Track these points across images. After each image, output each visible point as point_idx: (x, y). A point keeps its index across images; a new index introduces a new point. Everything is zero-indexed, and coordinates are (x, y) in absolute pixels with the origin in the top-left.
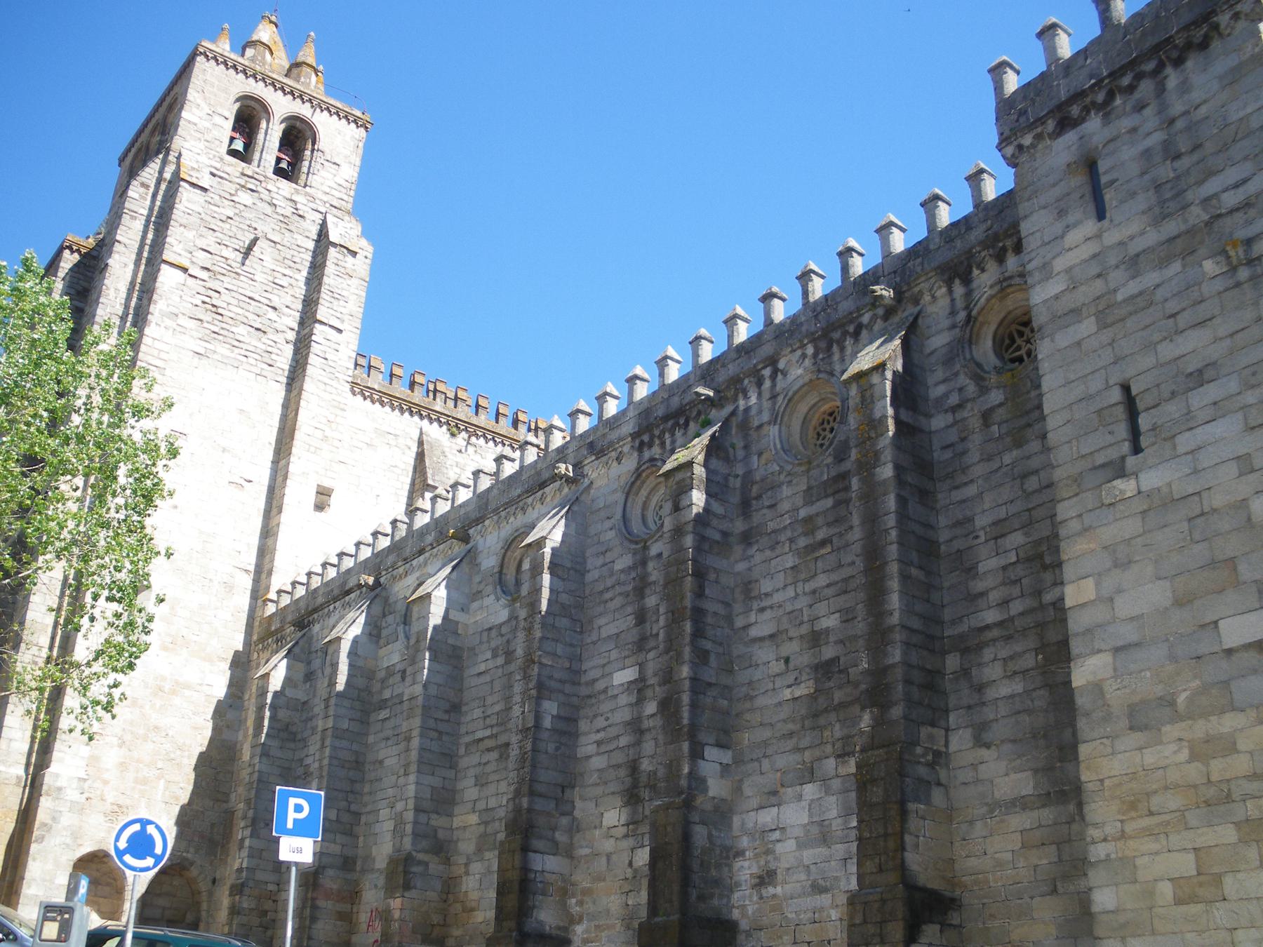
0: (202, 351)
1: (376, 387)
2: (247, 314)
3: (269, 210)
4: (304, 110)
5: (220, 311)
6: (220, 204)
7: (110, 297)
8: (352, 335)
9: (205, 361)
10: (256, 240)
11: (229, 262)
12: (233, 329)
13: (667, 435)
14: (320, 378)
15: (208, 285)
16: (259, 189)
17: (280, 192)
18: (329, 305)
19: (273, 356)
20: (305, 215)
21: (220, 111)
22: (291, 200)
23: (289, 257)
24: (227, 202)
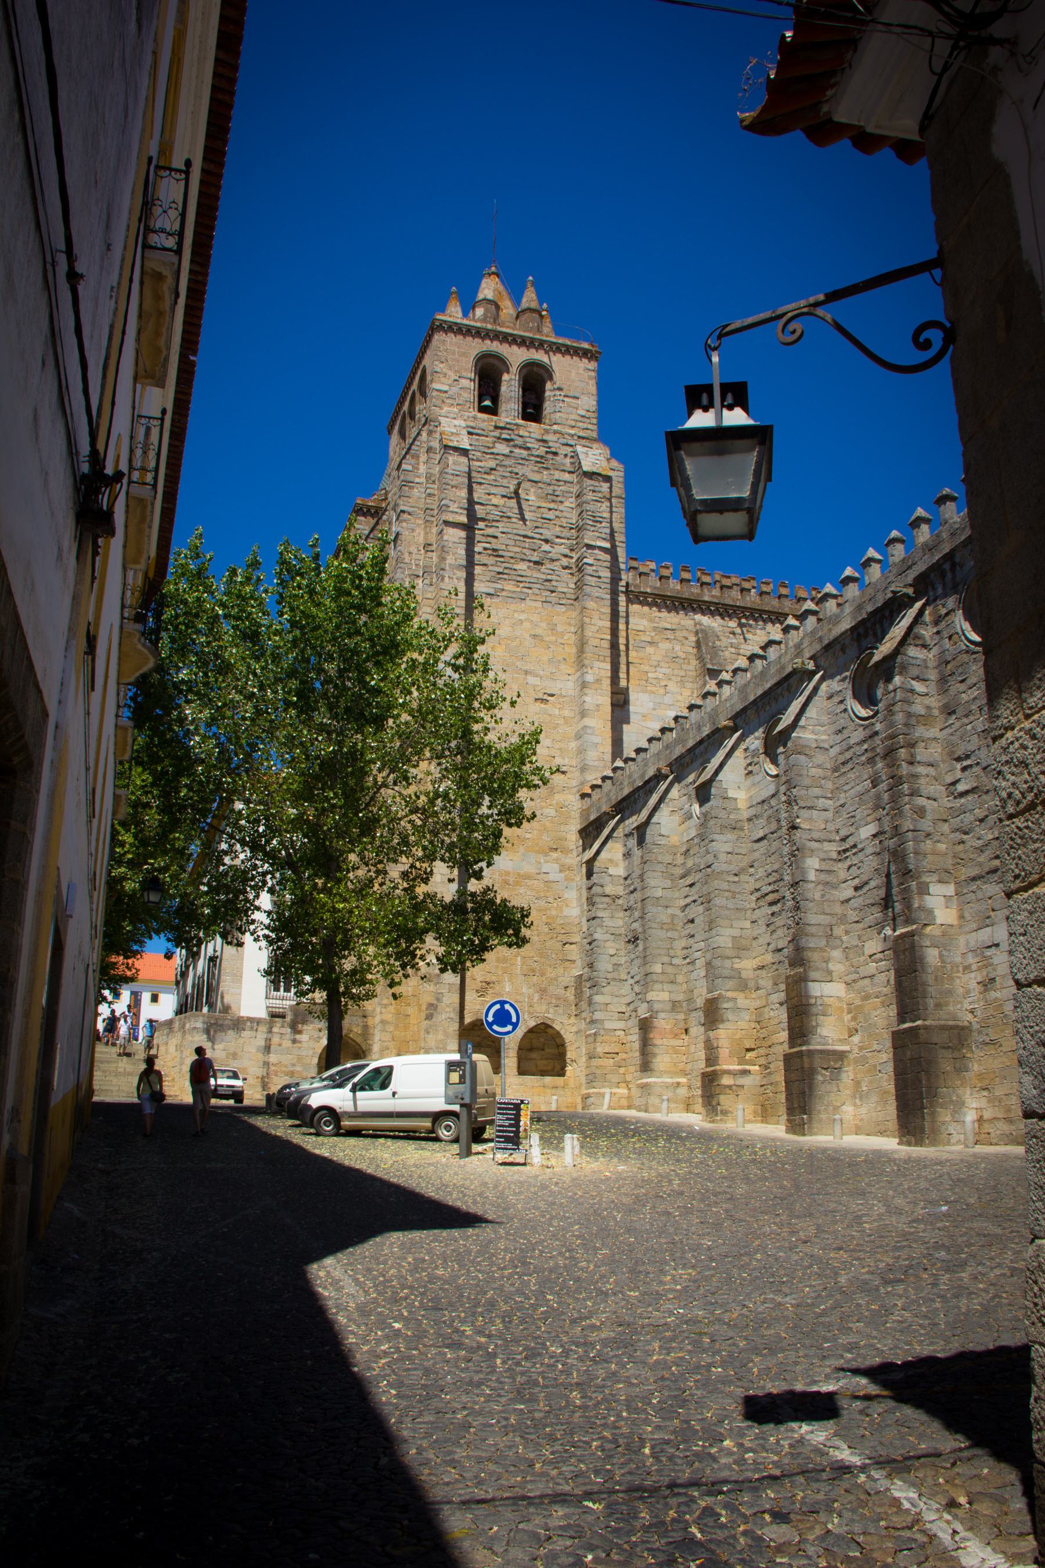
0: (492, 591)
1: (648, 590)
2: (524, 551)
4: (540, 356)
5: (500, 553)
7: (406, 560)
9: (495, 600)
10: (519, 484)
12: (515, 567)
13: (878, 626)
17: (533, 435)
18: (592, 529)
19: (554, 583)
20: (558, 451)
23: (551, 492)
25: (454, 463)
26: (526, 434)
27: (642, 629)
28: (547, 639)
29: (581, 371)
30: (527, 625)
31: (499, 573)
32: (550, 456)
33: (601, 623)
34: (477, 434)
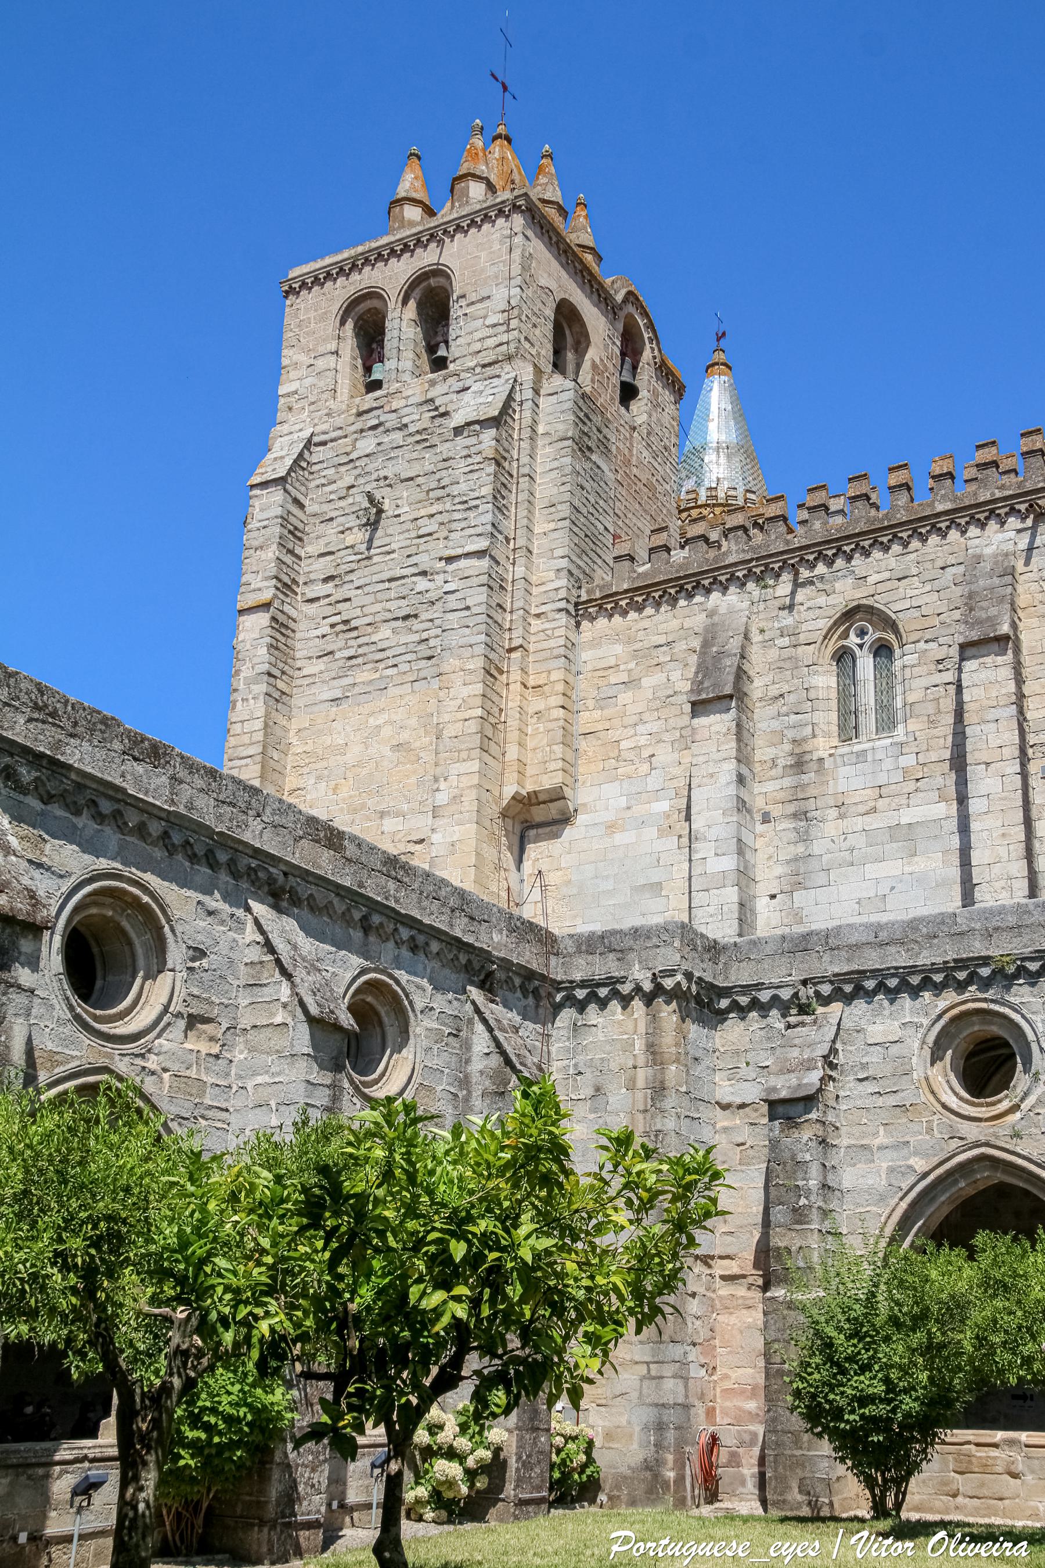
3: (397, 437)
4: (426, 258)
5: (354, 623)
6: (336, 477)
8: (556, 535)
9: (345, 705)
11: (356, 550)
12: (374, 638)
14: (463, 641)
15: (332, 599)
16: (382, 419)
17: (411, 401)
18: (463, 524)
21: (321, 349)
22: (426, 402)
23: (434, 485)
24: (343, 469)
25: (262, 510)
26: (403, 402)
27: (612, 662)
28: (417, 744)
29: (496, 246)
30: (387, 731)
31: (350, 658)
32: (438, 421)
33: (466, 691)
34: (332, 441)
